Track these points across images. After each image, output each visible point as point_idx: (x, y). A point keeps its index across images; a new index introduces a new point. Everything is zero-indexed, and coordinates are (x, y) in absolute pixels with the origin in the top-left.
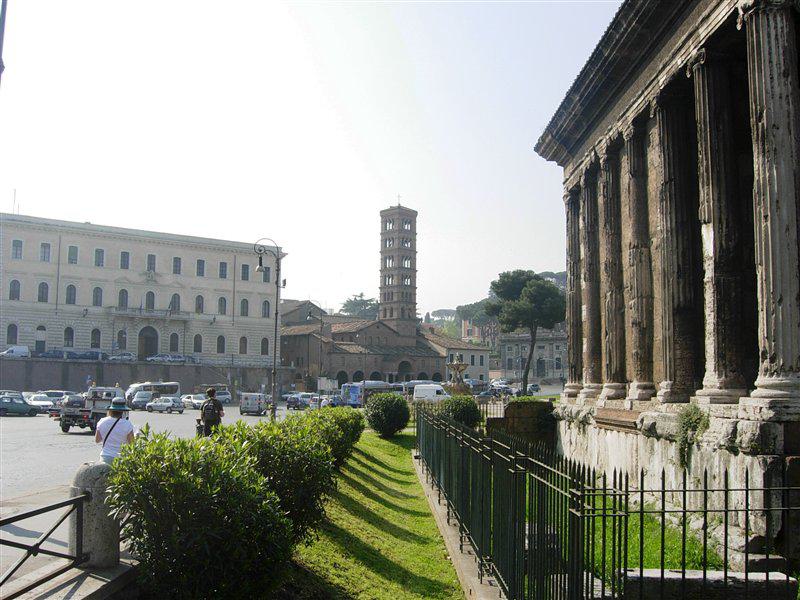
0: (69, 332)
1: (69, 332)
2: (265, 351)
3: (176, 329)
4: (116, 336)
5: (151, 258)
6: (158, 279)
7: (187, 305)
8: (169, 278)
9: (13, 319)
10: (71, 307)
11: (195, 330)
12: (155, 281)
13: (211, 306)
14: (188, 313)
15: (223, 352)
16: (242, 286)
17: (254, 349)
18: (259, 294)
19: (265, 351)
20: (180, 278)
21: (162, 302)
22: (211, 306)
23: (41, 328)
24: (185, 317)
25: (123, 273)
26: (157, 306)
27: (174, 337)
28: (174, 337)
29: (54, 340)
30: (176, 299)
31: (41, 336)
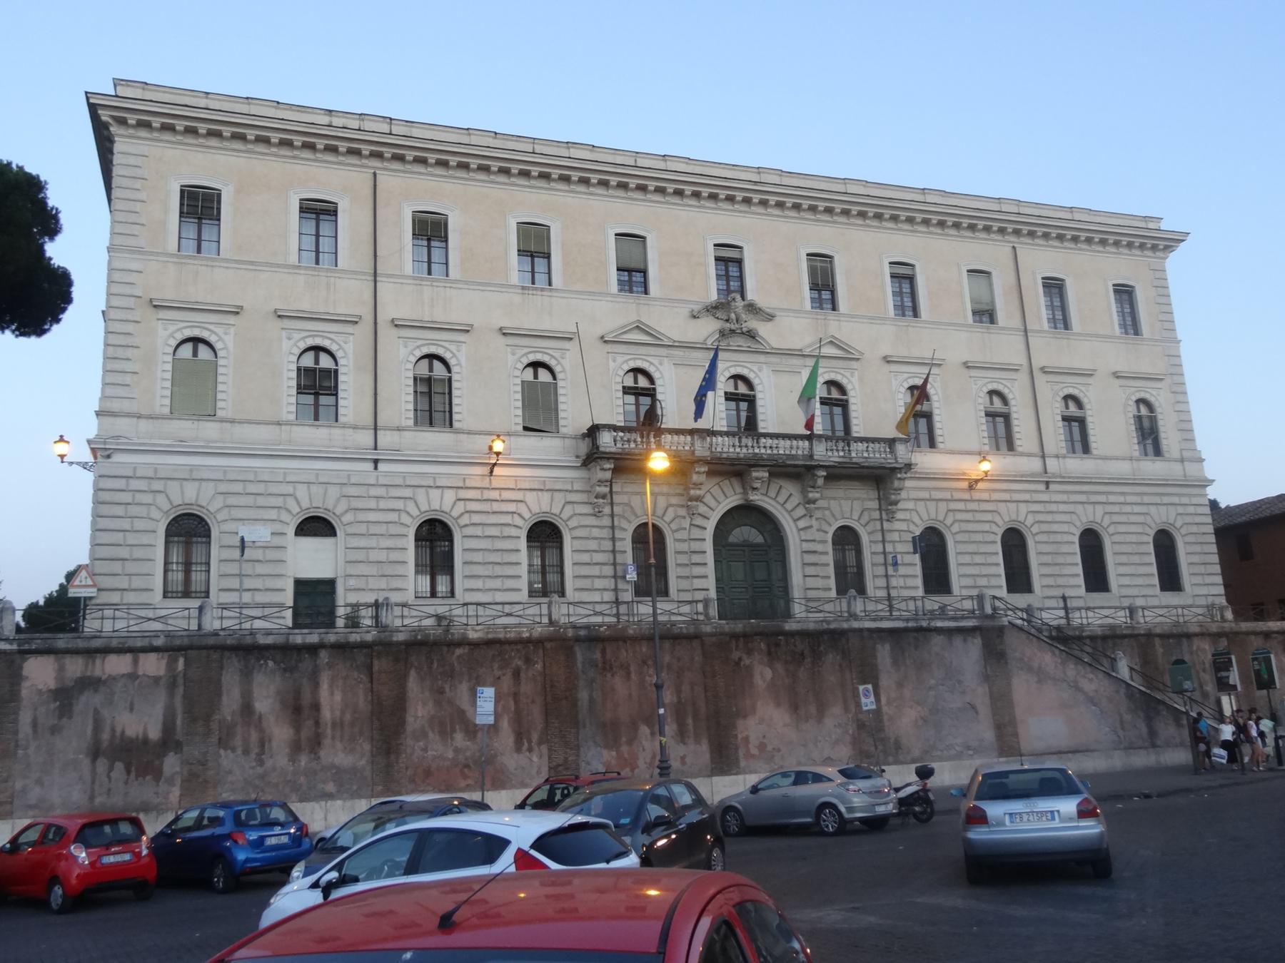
0: (435, 538)
1: (435, 538)
2: (1170, 578)
4: (626, 545)
5: (730, 263)
6: (763, 329)
8: (793, 325)
11: (914, 512)
12: (751, 335)
14: (891, 442)
16: (1049, 350)
17: (1132, 572)
18: (1117, 375)
19: (1170, 578)
20: (838, 327)
23: (316, 526)
24: (877, 456)
26: (767, 422)
27: (846, 538)
28: (846, 538)
29: (377, 578)
31: (314, 559)
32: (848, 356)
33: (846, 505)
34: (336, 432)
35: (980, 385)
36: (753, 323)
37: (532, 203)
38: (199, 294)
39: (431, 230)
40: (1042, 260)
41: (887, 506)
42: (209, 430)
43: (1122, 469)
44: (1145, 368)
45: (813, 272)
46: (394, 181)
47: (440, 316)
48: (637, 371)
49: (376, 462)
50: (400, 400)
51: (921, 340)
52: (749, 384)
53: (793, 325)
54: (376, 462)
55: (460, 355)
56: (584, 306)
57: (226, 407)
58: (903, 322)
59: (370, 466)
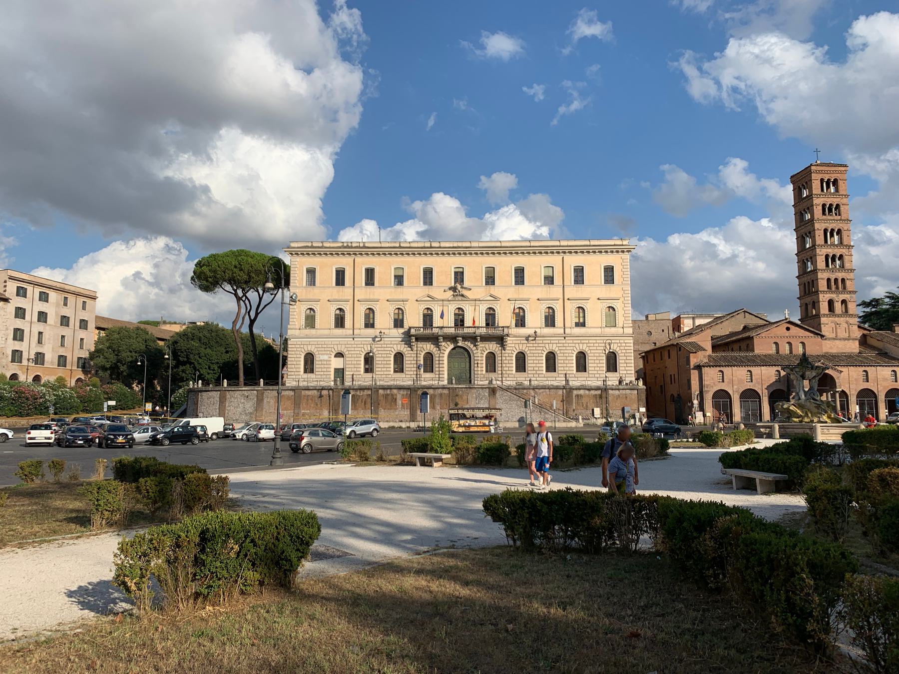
3: (493, 347)
7: (505, 318)
9: (311, 349)
10: (370, 331)
13: (535, 320)
15: (312, 371)
16: (573, 291)
20: (493, 290)
21: (475, 317)
22: (535, 320)
23: (340, 355)
25: (427, 290)
30: (491, 317)
32: (496, 299)
33: (491, 346)
35: (544, 306)
36: (465, 292)
37: (398, 261)
38: (311, 297)
39: (370, 273)
42: (313, 331)
43: (598, 331)
44: (613, 296)
45: (487, 272)
46: (359, 259)
47: (372, 297)
48: (428, 309)
50: (361, 321)
51: (523, 291)
52: (463, 311)
55: (377, 308)
56: (414, 290)
57: (317, 326)
58: (518, 286)
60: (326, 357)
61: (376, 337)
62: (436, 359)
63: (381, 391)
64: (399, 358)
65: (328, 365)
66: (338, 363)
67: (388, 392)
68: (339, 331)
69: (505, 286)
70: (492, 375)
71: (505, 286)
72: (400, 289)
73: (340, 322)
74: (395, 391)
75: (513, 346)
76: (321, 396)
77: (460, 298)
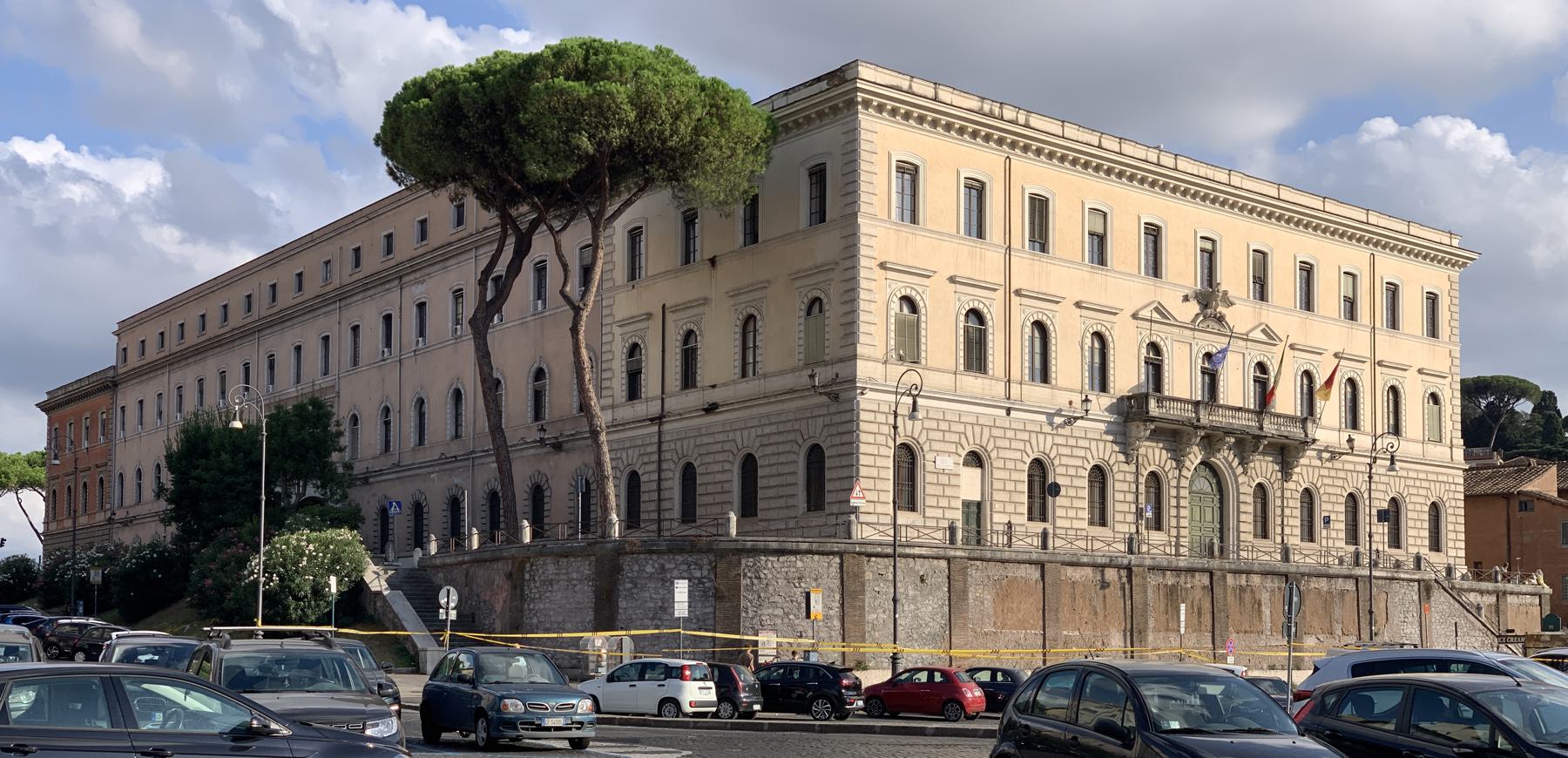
3: (1264, 468)
12: (1220, 319)
23: (975, 459)
34: (987, 382)
40: (1391, 267)
41: (1286, 470)
49: (1009, 411)
50: (1021, 362)
53: (1241, 314)
54: (1009, 411)
59: (1004, 412)
60: (946, 463)
61: (1059, 413)
62: (1169, 492)
63: (1230, 577)
64: (1099, 475)
65: (951, 484)
66: (969, 485)
67: (1243, 580)
68: (973, 383)
69: (1282, 312)
70: (904, 518)
71: (1282, 312)
72: (1099, 275)
73: (975, 356)
74: (1256, 579)
75: (1307, 470)
76: (1104, 585)
77: (1214, 325)
